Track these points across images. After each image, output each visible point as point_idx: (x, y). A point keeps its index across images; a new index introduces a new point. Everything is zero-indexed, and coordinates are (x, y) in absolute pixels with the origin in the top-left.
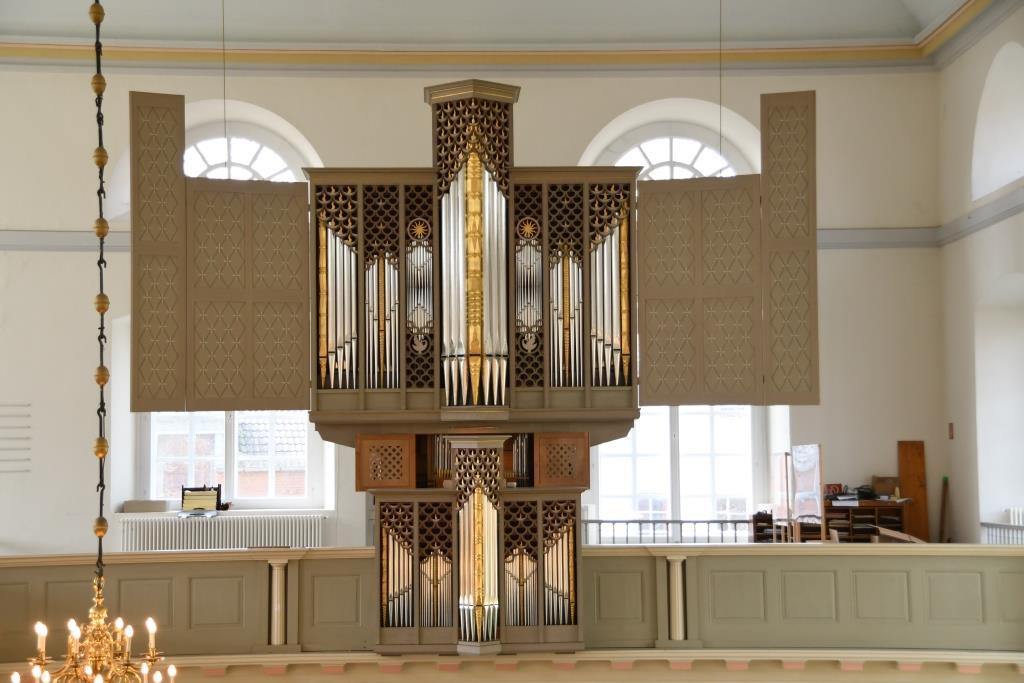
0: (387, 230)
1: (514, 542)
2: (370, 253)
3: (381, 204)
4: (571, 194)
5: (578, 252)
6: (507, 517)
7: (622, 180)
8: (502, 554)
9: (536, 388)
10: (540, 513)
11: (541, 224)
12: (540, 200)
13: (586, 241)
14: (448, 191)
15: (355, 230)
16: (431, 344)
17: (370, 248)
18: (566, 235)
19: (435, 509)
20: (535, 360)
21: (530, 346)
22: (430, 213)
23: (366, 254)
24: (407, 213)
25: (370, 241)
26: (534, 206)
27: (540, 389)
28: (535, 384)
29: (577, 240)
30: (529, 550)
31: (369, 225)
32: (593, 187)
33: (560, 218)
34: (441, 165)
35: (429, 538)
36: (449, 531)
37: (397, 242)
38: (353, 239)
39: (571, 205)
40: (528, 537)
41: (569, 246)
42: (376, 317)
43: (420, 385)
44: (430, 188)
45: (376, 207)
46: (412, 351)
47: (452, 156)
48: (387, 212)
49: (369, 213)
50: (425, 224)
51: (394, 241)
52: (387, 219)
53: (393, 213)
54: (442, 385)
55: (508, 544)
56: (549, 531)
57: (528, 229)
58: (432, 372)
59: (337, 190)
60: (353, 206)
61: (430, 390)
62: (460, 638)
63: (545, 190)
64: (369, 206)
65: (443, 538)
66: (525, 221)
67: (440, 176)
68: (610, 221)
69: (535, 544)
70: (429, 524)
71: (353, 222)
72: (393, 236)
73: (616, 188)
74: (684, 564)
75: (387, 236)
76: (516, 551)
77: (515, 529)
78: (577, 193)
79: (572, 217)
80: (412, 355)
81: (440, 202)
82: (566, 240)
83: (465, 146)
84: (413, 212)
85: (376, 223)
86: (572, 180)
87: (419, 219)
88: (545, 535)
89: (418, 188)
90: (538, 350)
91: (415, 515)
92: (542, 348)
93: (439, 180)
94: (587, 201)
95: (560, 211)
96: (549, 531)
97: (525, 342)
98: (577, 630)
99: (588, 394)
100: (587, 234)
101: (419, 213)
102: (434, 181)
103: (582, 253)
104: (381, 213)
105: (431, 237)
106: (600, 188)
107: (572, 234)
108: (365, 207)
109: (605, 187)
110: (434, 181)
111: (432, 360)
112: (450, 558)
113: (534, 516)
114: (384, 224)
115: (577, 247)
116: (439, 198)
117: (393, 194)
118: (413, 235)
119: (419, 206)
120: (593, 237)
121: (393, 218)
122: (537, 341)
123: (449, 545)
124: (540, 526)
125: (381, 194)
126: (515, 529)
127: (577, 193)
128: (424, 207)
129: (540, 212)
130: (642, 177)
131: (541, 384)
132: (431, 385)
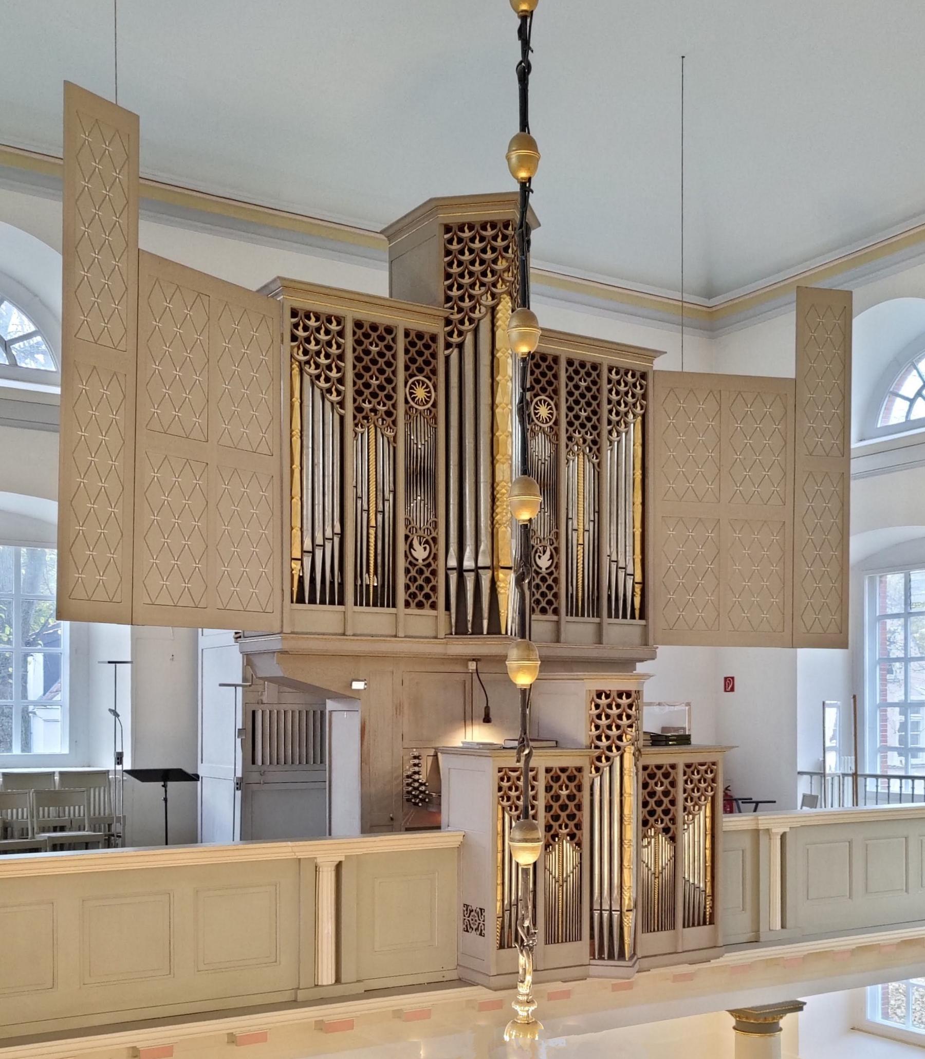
0: (381, 388)
1: (652, 820)
2: (359, 416)
3: (373, 349)
4: (588, 374)
5: (595, 448)
6: (645, 786)
7: (638, 364)
8: (640, 836)
9: (552, 617)
10: (681, 779)
11: (556, 405)
12: (556, 376)
13: (605, 433)
14: (460, 346)
15: (341, 381)
16: (434, 551)
17: (359, 409)
18: (583, 426)
19: (564, 776)
20: (550, 581)
21: (544, 562)
22: (434, 372)
23: (355, 417)
24: (407, 368)
25: (360, 399)
26: (550, 383)
27: (555, 618)
28: (550, 611)
29: (595, 433)
30: (572, 836)
31: (359, 376)
32: (610, 371)
33: (577, 402)
34: (452, 308)
35: (556, 818)
36: (579, 807)
37: (394, 406)
38: (339, 393)
39: (588, 389)
40: (666, 812)
41: (585, 441)
42: (365, 507)
43: (420, 605)
44: (434, 338)
45: (367, 352)
46: (410, 558)
47: (471, 297)
48: (381, 361)
49: (358, 359)
50: (427, 387)
51: (389, 403)
52: (382, 372)
53: (389, 364)
54: (448, 608)
55: (645, 823)
56: (689, 804)
57: (543, 411)
58: (434, 589)
59: (317, 320)
60: (339, 347)
61: (433, 612)
62: (592, 954)
63: (563, 364)
64: (359, 349)
65: (571, 817)
66: (540, 401)
67: (448, 322)
68: (626, 414)
69: (673, 820)
70: (557, 798)
71: (339, 370)
72: (389, 397)
73: (633, 376)
74: (783, 836)
75: (382, 394)
76: (652, 832)
77: (652, 802)
78: (594, 374)
79: (589, 404)
80: (411, 563)
81: (447, 358)
82: (583, 431)
83: (494, 285)
84: (413, 367)
85: (367, 375)
86: (591, 356)
87: (420, 377)
88: (685, 809)
89: (420, 336)
90: (553, 568)
91: (541, 785)
92: (557, 567)
93: (448, 329)
94: (606, 387)
95: (577, 393)
96: (689, 804)
97: (540, 557)
98: (716, 931)
99: (605, 626)
100: (605, 428)
101: (420, 370)
102: (439, 329)
103: (598, 450)
104: (374, 362)
105: (434, 405)
106: (617, 373)
107: (589, 425)
108: (354, 350)
109: (622, 372)
110: (439, 329)
111: (434, 573)
112: (579, 844)
113: (673, 784)
114: (377, 379)
115: (594, 442)
116: (447, 352)
117: (389, 338)
118: (413, 399)
119: (420, 360)
120: (610, 432)
121: (389, 371)
122: (552, 557)
123: (578, 826)
124: (681, 797)
125: (374, 335)
126: (556, 806)
127: (594, 374)
128: (427, 363)
129: (556, 392)
130: (659, 364)
131: (556, 612)
132: (433, 606)
